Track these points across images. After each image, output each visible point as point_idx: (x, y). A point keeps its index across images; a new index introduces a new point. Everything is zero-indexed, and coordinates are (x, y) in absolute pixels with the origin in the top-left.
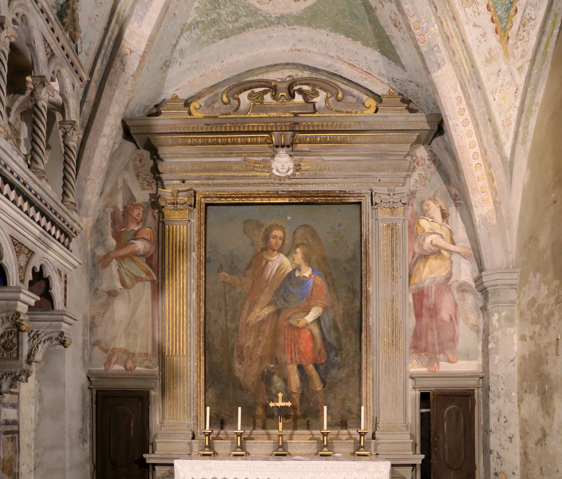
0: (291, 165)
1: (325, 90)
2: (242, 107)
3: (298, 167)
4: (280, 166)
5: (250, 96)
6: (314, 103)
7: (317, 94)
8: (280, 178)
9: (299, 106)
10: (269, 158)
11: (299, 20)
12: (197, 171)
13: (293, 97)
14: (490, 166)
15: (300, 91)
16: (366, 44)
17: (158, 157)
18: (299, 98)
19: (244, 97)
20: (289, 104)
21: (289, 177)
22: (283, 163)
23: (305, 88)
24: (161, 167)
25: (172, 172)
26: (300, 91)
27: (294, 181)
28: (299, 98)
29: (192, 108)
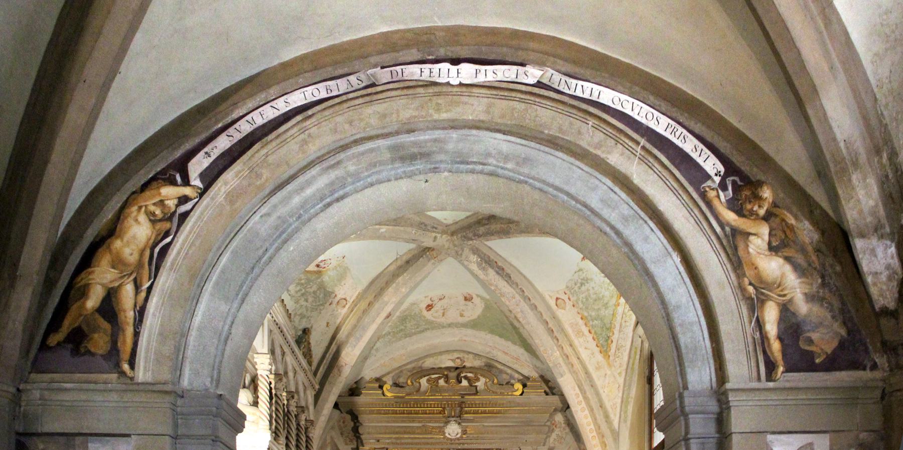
0: (460, 431)
1: (484, 377)
2: (423, 389)
3: (464, 432)
4: (451, 432)
5: (428, 381)
6: (476, 387)
7: (478, 380)
8: (451, 440)
9: (465, 388)
10: (442, 425)
11: (464, 325)
12: (389, 433)
13: (461, 382)
14: (603, 436)
15: (466, 378)
16: (515, 343)
17: (358, 421)
18: (465, 383)
19: (424, 381)
20: (458, 387)
21: (458, 439)
22: (453, 430)
23: (469, 375)
24: (361, 430)
25: (369, 433)
26: (466, 378)
27: (461, 441)
28: (465, 383)
29: (384, 389)
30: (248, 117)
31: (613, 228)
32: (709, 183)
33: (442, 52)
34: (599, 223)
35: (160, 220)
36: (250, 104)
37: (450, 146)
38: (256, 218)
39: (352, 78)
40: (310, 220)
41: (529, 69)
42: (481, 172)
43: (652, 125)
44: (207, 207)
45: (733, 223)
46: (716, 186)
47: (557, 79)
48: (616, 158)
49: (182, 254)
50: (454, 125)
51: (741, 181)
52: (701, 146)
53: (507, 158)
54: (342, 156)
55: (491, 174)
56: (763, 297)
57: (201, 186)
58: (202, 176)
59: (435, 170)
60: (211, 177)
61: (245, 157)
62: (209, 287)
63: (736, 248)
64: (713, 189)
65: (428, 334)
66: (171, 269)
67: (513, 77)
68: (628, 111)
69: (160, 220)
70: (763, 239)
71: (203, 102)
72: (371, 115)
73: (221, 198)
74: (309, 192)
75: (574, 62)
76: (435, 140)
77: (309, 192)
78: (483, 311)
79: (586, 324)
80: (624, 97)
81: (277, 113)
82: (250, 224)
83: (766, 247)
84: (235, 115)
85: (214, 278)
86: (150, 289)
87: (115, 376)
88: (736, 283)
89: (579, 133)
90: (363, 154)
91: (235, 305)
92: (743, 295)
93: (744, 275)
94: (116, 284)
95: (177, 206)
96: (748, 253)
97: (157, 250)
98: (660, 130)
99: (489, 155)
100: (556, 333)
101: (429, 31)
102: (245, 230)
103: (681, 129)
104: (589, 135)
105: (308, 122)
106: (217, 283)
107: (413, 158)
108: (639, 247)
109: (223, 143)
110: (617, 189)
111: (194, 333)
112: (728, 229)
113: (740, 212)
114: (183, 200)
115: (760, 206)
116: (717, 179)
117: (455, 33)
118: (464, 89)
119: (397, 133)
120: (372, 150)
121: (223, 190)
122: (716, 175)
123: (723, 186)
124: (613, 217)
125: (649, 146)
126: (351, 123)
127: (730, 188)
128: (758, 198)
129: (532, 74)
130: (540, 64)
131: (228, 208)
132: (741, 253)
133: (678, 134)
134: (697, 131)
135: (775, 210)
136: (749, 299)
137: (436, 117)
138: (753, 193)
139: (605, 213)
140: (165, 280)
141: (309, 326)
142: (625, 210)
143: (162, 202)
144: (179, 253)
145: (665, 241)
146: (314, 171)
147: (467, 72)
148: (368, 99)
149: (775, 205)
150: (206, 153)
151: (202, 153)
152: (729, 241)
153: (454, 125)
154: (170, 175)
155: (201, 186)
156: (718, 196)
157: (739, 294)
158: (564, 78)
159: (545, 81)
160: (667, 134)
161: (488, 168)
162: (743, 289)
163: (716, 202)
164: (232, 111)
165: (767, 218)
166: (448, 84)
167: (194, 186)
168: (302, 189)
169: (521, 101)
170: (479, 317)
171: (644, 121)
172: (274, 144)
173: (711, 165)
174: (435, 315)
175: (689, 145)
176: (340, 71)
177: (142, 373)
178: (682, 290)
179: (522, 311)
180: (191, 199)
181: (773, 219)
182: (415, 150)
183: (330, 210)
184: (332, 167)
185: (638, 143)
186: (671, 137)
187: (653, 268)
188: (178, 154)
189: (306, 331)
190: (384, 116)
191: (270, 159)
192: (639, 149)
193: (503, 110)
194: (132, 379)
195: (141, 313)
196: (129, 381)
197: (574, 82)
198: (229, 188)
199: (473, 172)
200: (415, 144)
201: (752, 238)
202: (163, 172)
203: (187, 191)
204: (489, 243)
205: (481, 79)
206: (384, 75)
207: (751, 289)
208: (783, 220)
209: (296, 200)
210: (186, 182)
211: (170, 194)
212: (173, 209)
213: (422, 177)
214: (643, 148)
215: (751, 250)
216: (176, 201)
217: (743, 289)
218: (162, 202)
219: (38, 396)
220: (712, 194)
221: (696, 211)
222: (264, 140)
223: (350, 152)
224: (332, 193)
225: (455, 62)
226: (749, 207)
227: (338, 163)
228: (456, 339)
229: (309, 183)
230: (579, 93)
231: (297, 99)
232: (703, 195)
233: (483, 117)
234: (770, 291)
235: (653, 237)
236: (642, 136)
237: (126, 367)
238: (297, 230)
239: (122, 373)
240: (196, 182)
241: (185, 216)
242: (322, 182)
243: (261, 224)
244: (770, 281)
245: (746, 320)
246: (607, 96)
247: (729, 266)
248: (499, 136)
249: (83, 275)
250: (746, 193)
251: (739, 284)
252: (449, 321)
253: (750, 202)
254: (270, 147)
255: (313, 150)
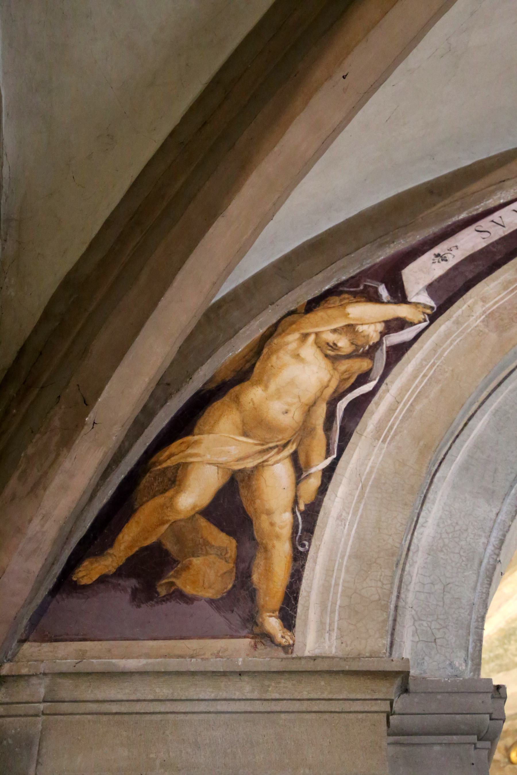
35: (349, 356)
44: (448, 335)
57: (432, 304)
58: (432, 289)
60: (448, 292)
69: (349, 356)
73: (476, 321)
86: (328, 473)
87: (247, 642)
94: (250, 464)
95: (383, 334)
97: (342, 405)
109: (469, 242)
114: (398, 324)
121: (479, 309)
131: (493, 336)
140: (364, 455)
144: (391, 410)
150: (438, 255)
151: (429, 256)
154: (366, 286)
155: (432, 304)
167: (417, 304)
177: (314, 637)
180: (412, 324)
194: (287, 648)
195: (308, 519)
196: (282, 655)
198: (491, 305)
202: (353, 281)
203: (402, 311)
210: (399, 295)
211: (368, 316)
212: (375, 338)
216: (380, 327)
219: (42, 691)
237: (273, 624)
239: (267, 637)
241: (398, 352)
249: (174, 447)
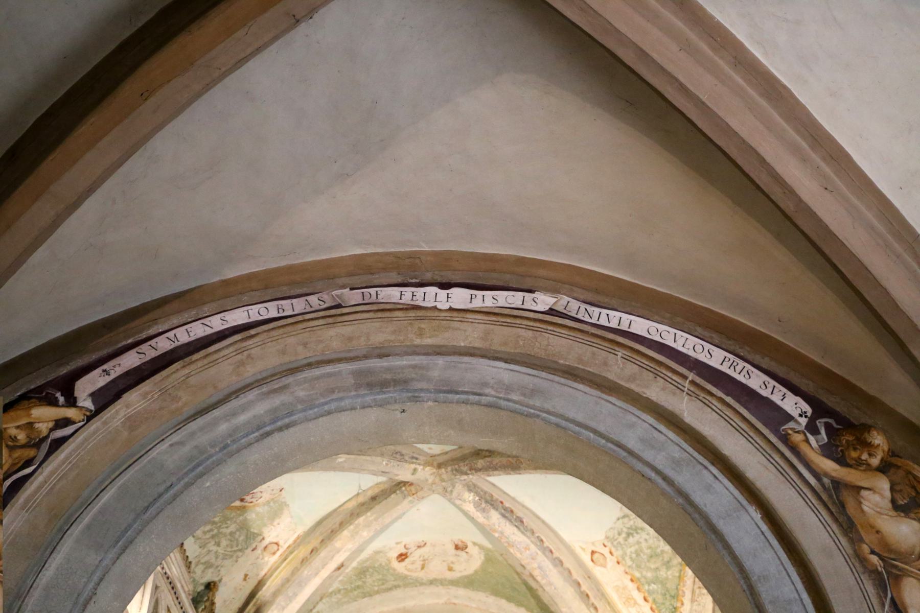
30: (171, 334)
31: (658, 472)
32: (791, 425)
33: (428, 276)
34: (639, 466)
35: (23, 447)
36: (175, 321)
37: (435, 374)
38: (164, 446)
39: (313, 299)
40: (238, 451)
41: (539, 296)
42: (478, 404)
43: (703, 358)
45: (834, 474)
46: (803, 428)
47: (574, 307)
48: (656, 392)
49: (44, 491)
50: (439, 351)
51: (837, 423)
52: (773, 383)
53: (509, 388)
54: (290, 379)
55: (489, 405)
56: (894, 571)
57: (92, 408)
58: (94, 395)
59: (415, 399)
60: (106, 398)
61: (157, 377)
62: (76, 530)
63: (842, 506)
64: (798, 432)
65: (397, 593)
66: (22, 508)
67: (518, 304)
68: (669, 342)
69: (23, 447)
70: (882, 496)
71: (112, 316)
72: (333, 337)
74: (242, 418)
75: (597, 291)
76: (414, 367)
77: (242, 418)
78: (483, 564)
79: (638, 589)
80: (662, 327)
81: (209, 331)
82: (153, 454)
83: (890, 505)
84: (152, 332)
85: (87, 519)
88: (850, 551)
89: (605, 364)
90: (318, 378)
91: (111, 555)
92: (864, 567)
93: (861, 540)
95: (51, 430)
96: (863, 511)
98: (714, 363)
99: (485, 384)
100: (592, 599)
101: (412, 255)
102: (145, 460)
103: (742, 364)
104: (618, 367)
105: (250, 342)
106: (88, 527)
107: (384, 385)
108: (698, 497)
109: (130, 361)
110: (662, 427)
111: (36, 594)
112: (826, 481)
113: (842, 461)
115: (870, 455)
116: (803, 421)
117: (445, 258)
118: (455, 314)
119: (366, 357)
120: (330, 375)
122: (801, 416)
123: (812, 428)
124: (660, 461)
125: (699, 380)
126: (305, 345)
127: (823, 431)
128: (868, 446)
129: (543, 301)
130: (553, 291)
132: (851, 509)
133: (738, 368)
134: (764, 366)
135: (894, 460)
136: (874, 573)
137: (418, 341)
138: (858, 439)
139: (648, 455)
141: (216, 579)
142: (677, 453)
143: (30, 425)
145: (736, 493)
146: (251, 395)
147: (460, 297)
148: (330, 320)
149: (892, 453)
150: (104, 371)
151: (98, 371)
152: (830, 496)
153: (439, 351)
154: (47, 393)
155: (92, 408)
156: (807, 441)
157: (857, 564)
158: (583, 306)
159: (560, 308)
160: (724, 368)
161: (484, 399)
162: (862, 560)
163: (804, 448)
164: (149, 327)
165: (884, 468)
166: (435, 308)
167: (82, 408)
168: (234, 414)
169: (528, 328)
170: (476, 572)
171: (691, 353)
172: (200, 364)
173: (792, 404)
174: (410, 567)
175: (756, 381)
176: (299, 291)
178: (769, 555)
179: (540, 568)
180: (74, 423)
181: (892, 470)
182: (388, 376)
183: (269, 440)
184: (275, 391)
185: (685, 378)
186: (730, 372)
187: (721, 525)
188: (63, 371)
189: (210, 587)
190: (350, 339)
191: (192, 381)
192: (687, 384)
193: (502, 336)
197: (597, 310)
199: (465, 402)
200: (388, 370)
201: (864, 493)
203: (71, 413)
204: (491, 479)
205: (477, 304)
206: (355, 297)
207: (874, 559)
208: (909, 473)
209: (223, 428)
210: (71, 402)
211: (43, 416)
212: (45, 432)
213: (397, 406)
214: (693, 382)
215: (865, 508)
216: (51, 425)
217: (862, 560)
218: (30, 425)
220: (797, 438)
221: (777, 458)
222: (187, 360)
223: (301, 376)
224: (274, 421)
225: (445, 286)
226: (854, 454)
227: (285, 387)
228: (442, 601)
229: (244, 408)
230: (603, 322)
231: (238, 317)
232: (785, 439)
233: (478, 344)
234: (906, 564)
235: (717, 486)
236: (690, 369)
238: (219, 463)
240: (87, 403)
241: (58, 444)
242: (261, 408)
243: (168, 454)
244: (903, 550)
245: (875, 601)
246: (640, 326)
247: (834, 527)
248: (501, 364)
250: (848, 438)
251: (855, 551)
252: (432, 576)
253: (855, 449)
254: (193, 367)
255: (251, 372)
